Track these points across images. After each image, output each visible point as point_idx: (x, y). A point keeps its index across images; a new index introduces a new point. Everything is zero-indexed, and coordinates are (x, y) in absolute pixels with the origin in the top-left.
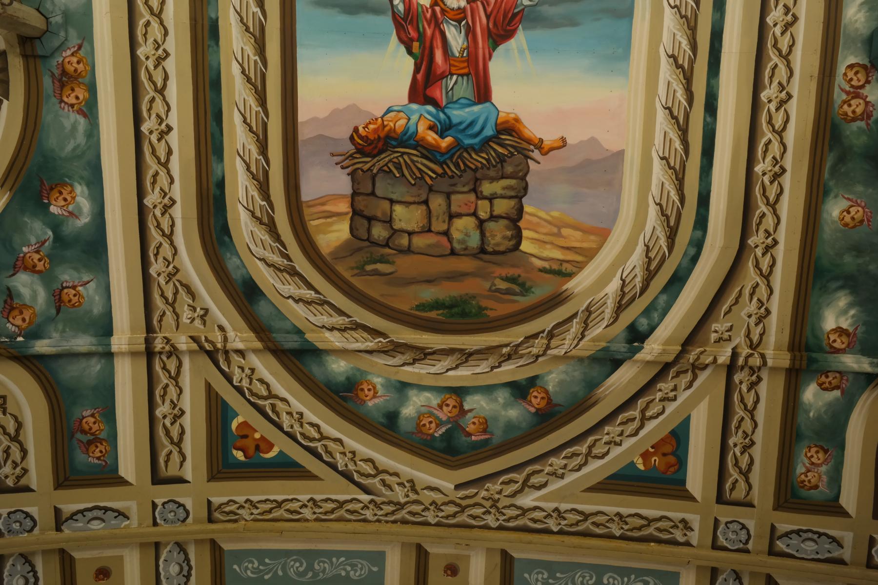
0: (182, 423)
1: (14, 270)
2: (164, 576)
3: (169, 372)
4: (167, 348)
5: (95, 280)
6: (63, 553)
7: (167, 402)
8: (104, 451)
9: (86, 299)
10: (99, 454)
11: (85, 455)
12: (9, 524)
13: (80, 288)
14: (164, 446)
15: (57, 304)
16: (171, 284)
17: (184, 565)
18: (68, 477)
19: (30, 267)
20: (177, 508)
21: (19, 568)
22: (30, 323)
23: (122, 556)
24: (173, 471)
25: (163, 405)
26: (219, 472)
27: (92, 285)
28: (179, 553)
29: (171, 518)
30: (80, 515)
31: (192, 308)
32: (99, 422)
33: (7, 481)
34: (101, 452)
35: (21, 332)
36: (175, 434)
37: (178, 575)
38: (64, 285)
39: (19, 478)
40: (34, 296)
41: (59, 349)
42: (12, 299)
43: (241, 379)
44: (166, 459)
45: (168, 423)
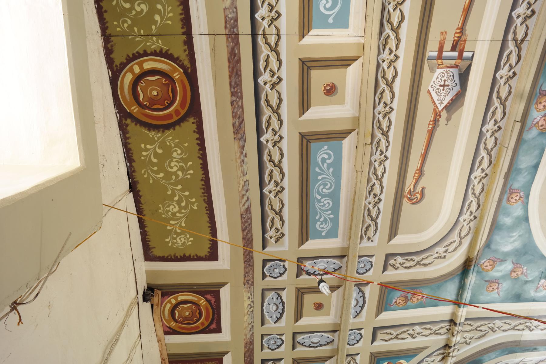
0: (408, 338)
1: (515, 263)
2: (312, 336)
3: (438, 330)
4: (456, 332)
5: (499, 297)
6: (337, 287)
7: (422, 331)
8: (400, 304)
9: (490, 293)
10: (398, 302)
11: (399, 295)
12: (364, 262)
13: (496, 291)
14: (396, 332)
15: (490, 281)
16: (488, 329)
17: (318, 344)
18: (387, 289)
19: (515, 270)
20: (357, 340)
21: (333, 266)
22: (483, 269)
23: (329, 315)
24: (380, 335)
25: (421, 329)
26: (375, 357)
27: (497, 296)
28: (326, 342)
29: (351, 337)
30: (362, 295)
31: (471, 338)
32: (418, 301)
33: (393, 260)
34: (399, 303)
35: (479, 265)
36: (403, 336)
37: (311, 342)
38: (500, 284)
39: (393, 266)
40: (497, 271)
41: (468, 286)
42: (499, 262)
43: (427, 362)
44: (388, 333)
45: (409, 332)
